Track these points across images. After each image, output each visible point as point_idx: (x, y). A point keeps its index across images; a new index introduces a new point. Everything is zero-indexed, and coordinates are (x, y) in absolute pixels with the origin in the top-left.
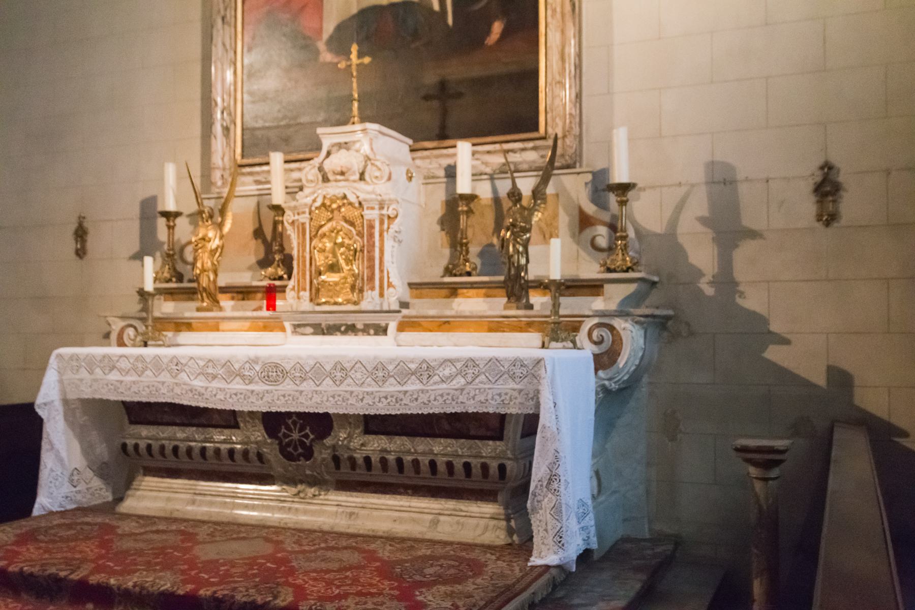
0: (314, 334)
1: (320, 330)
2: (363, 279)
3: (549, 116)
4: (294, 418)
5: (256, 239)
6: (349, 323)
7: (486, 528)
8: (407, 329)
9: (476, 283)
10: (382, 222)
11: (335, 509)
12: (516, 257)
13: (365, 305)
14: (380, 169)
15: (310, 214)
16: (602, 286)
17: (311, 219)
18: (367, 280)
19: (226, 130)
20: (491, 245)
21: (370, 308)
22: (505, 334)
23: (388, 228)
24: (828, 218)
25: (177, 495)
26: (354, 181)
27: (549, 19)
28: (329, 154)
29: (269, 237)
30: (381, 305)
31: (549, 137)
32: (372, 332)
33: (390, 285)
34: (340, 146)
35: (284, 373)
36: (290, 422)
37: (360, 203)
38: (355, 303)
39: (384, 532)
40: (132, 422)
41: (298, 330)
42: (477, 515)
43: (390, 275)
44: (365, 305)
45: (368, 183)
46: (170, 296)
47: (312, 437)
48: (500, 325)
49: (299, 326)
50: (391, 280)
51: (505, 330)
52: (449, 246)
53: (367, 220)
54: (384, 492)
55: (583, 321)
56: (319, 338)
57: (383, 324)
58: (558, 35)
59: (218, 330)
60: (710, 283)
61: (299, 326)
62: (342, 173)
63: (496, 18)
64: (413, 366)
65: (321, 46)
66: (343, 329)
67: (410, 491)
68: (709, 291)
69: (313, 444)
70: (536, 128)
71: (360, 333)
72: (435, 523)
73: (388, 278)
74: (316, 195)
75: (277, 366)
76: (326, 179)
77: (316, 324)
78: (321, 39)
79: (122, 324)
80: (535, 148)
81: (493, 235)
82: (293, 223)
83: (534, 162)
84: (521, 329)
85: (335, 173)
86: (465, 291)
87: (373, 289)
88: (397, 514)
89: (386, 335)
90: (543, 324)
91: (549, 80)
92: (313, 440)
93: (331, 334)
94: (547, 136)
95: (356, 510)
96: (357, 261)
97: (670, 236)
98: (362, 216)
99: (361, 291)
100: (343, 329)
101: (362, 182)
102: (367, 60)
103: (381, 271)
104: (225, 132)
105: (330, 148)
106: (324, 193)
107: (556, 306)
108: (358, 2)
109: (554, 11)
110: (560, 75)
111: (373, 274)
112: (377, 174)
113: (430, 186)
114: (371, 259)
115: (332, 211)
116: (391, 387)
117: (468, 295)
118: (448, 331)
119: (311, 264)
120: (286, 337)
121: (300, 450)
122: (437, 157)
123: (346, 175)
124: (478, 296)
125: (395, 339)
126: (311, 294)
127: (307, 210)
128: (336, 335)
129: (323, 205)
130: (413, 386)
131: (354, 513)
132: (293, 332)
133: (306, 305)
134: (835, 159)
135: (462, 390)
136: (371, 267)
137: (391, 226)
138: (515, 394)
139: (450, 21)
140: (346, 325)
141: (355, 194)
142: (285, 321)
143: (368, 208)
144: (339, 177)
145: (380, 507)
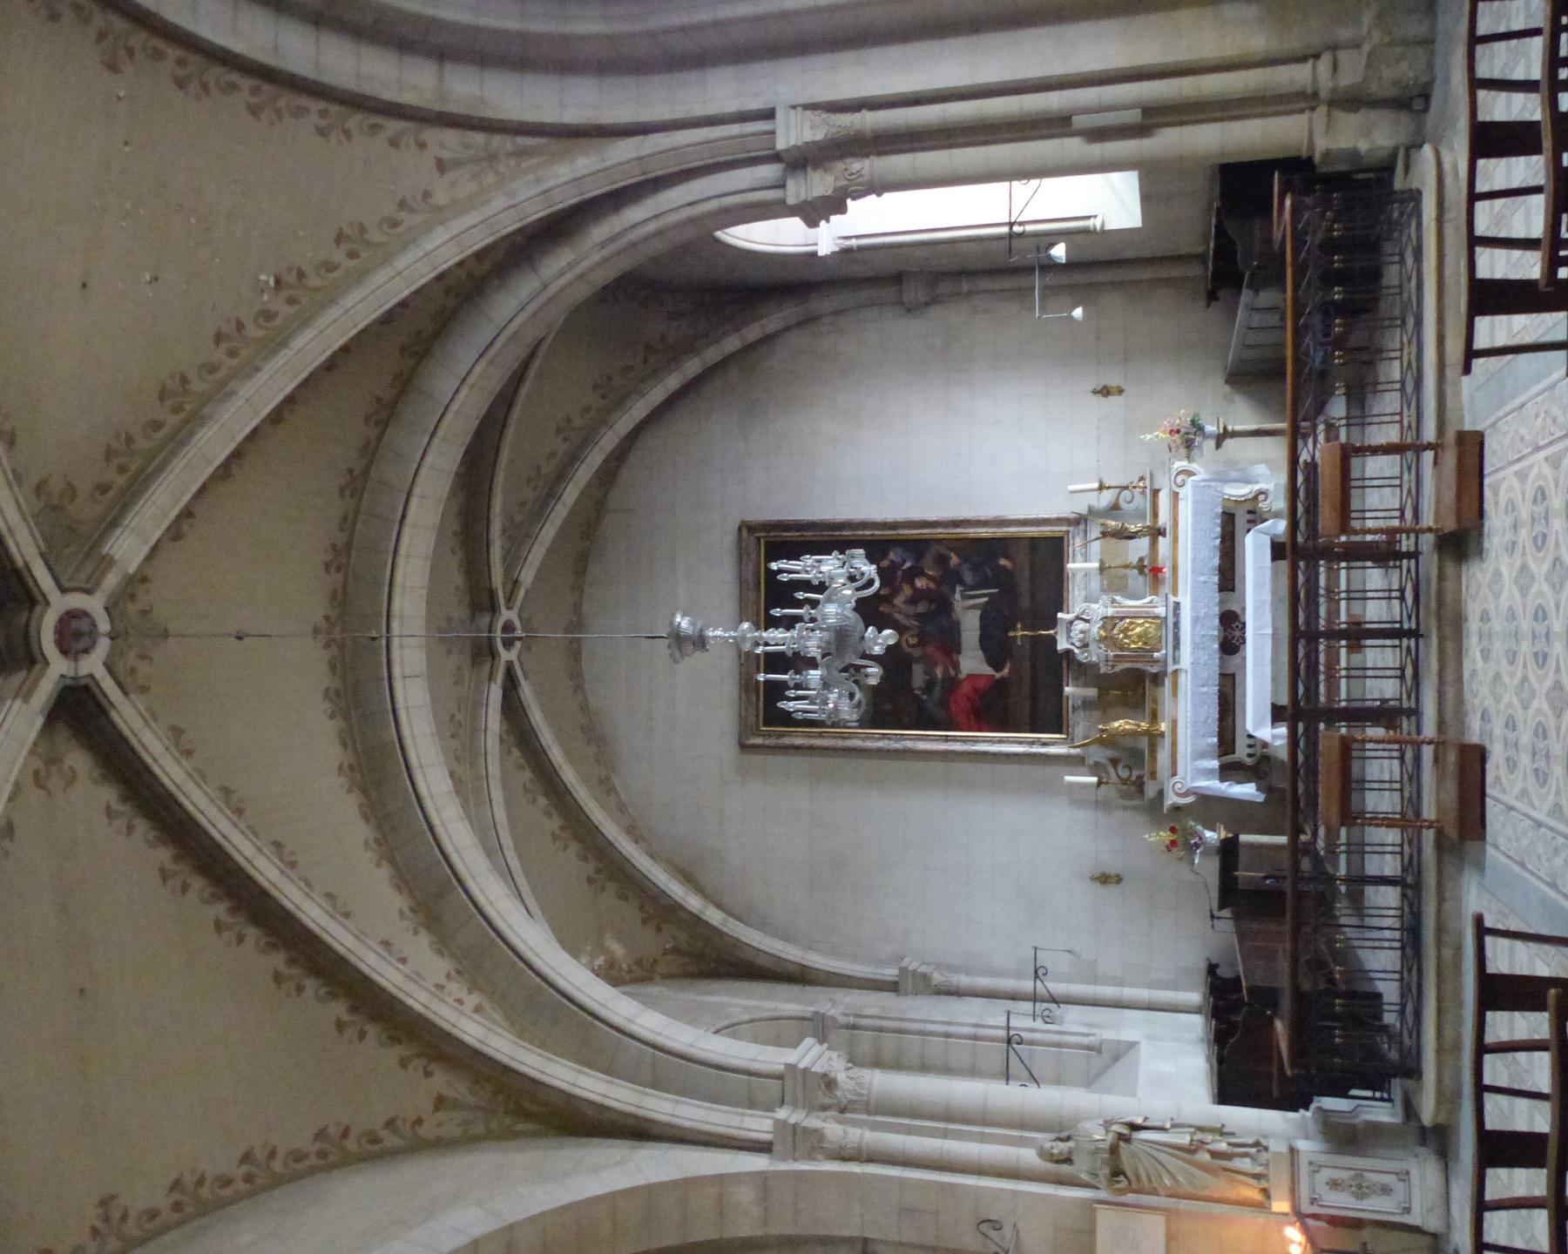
10: (1115, 607)
24: (1120, 391)
33: (1151, 602)
40: (1234, 753)
56: (1182, 647)
61: (1174, 659)
65: (998, 675)
80: (1073, 539)
82: (1113, 666)
102: (1019, 626)
103: (1143, 607)
134: (1092, 389)
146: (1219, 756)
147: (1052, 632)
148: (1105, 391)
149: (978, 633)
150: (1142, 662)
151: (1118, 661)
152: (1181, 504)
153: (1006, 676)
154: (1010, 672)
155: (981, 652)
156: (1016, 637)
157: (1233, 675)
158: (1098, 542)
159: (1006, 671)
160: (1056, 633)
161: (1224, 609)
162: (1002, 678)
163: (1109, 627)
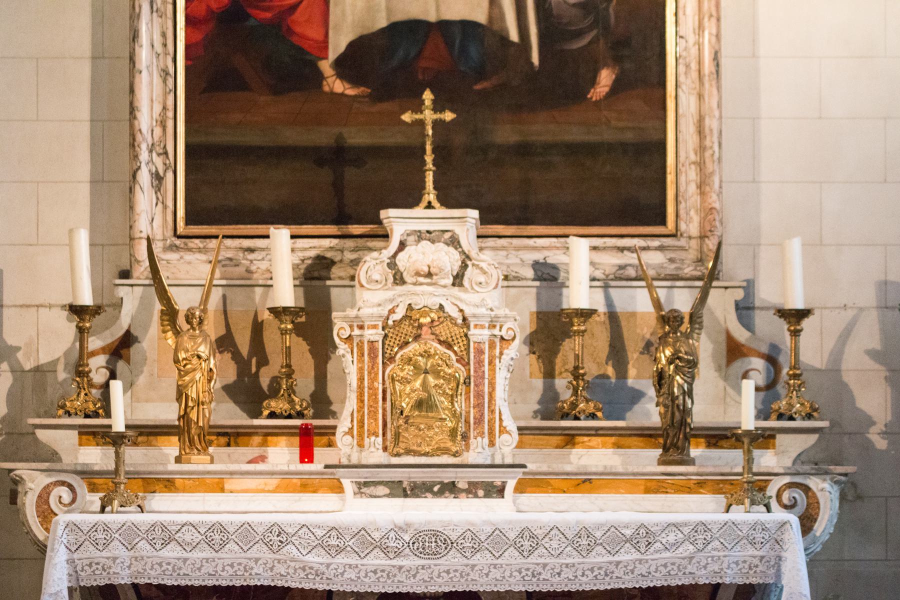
0: (391, 495)
1: (399, 490)
2: (467, 422)
3: (682, 206)
5: (220, 352)
6: (446, 481)
8: (529, 489)
9: (602, 428)
10: (492, 346)
12: (681, 397)
14: (485, 273)
15: (383, 329)
16: (773, 437)
17: (386, 336)
18: (475, 423)
19: (158, 178)
20: (605, 376)
21: (480, 461)
22: (668, 495)
23: (501, 354)
26: (445, 287)
27: (682, 79)
28: (402, 246)
29: (244, 349)
30: (493, 456)
31: (681, 235)
32: (481, 493)
33: (503, 430)
34: (420, 236)
35: (448, 544)
37: (464, 319)
41: (364, 490)
43: (503, 418)
44: (471, 457)
45: (466, 291)
46: (91, 438)
48: (659, 484)
49: (366, 484)
50: (504, 424)
51: (668, 490)
52: (542, 375)
53: (475, 342)
55: (771, 480)
56: (399, 502)
58: (693, 100)
59: (222, 490)
60: (884, 434)
61: (366, 484)
62: (429, 275)
63: (606, 65)
64: (628, 532)
65: (326, 67)
66: (436, 489)
68: (881, 444)
70: (663, 222)
71: (464, 494)
73: (501, 420)
74: (395, 304)
75: (436, 534)
76: (399, 279)
77: (393, 482)
78: (326, 58)
79: (44, 480)
80: (661, 248)
81: (607, 363)
82: (349, 338)
83: (661, 266)
84: (689, 490)
85: (418, 274)
86: (586, 439)
87: (482, 434)
89: (503, 497)
90: (718, 484)
91: (682, 158)
93: (418, 496)
94: (679, 233)
96: (459, 397)
97: (834, 371)
98: (466, 335)
99: (465, 437)
100: (436, 489)
101: (456, 288)
102: (449, 116)
103: (492, 412)
104: (155, 183)
105: (405, 237)
107: (749, 461)
108: (389, 10)
109: (688, 66)
110: (696, 154)
111: (482, 415)
112: (482, 279)
113: (512, 290)
114: (479, 395)
115: (420, 326)
116: (600, 557)
117: (590, 444)
119: (384, 399)
120: (343, 500)
122: (518, 249)
123: (434, 277)
124: (604, 446)
125: (514, 502)
126: (384, 440)
127: (380, 324)
128: (426, 497)
129: (406, 317)
130: (627, 555)
132: (355, 494)
133: (377, 455)
135: (691, 558)
136: (479, 406)
137: (505, 351)
138: (756, 561)
139: (535, 58)
140: (441, 483)
141: (458, 307)
142: (344, 478)
143: (476, 326)
144: (421, 279)
146: (135, 586)
147: (431, 195)
149: (432, 18)
150: (360, 408)
153: (326, 89)
154: (333, 94)
155: (382, 23)
156: (418, 108)
158: (651, 309)
159: (339, 86)
160: (429, 206)
162: (319, 77)
163: (444, 331)
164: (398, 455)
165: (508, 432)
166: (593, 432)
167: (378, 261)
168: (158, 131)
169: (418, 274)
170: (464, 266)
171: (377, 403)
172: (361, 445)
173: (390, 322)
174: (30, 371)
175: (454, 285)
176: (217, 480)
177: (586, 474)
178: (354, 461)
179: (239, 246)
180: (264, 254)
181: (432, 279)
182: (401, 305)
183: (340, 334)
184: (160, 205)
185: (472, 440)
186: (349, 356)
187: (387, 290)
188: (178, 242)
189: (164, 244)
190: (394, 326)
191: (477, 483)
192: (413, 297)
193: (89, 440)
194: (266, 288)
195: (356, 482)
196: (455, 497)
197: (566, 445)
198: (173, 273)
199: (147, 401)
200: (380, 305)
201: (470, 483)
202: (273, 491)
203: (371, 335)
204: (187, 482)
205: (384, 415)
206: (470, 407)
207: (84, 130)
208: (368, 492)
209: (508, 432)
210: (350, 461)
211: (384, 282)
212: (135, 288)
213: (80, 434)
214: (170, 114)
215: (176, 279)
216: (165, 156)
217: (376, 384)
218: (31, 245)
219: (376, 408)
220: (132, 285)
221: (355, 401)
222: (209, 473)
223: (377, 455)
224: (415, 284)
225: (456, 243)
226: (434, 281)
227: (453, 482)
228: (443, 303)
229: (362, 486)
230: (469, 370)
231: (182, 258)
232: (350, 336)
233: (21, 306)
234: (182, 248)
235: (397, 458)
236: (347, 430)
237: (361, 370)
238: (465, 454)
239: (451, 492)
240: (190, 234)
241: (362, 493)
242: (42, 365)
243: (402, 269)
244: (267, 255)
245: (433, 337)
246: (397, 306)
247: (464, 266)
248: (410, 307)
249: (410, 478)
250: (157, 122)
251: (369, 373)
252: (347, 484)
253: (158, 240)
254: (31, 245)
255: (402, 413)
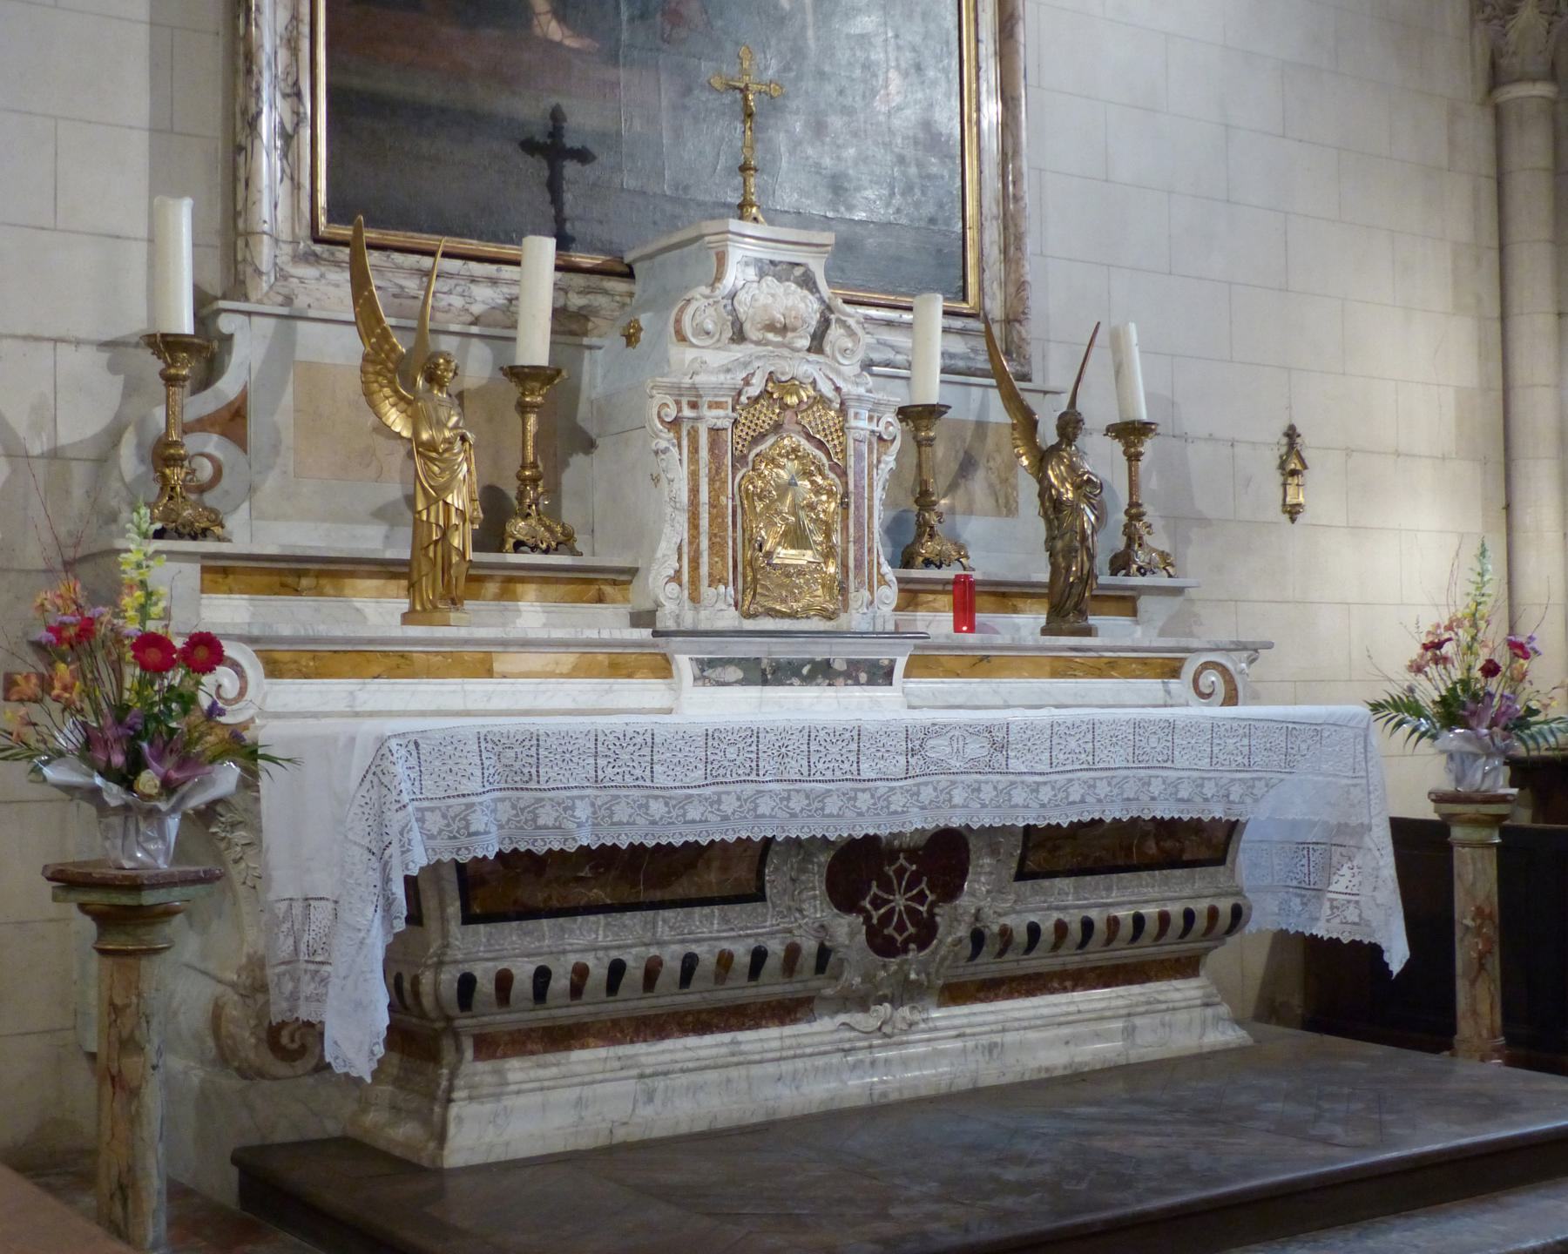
0: (745, 682)
4: (902, 861)
6: (819, 658)
7: (1204, 1022)
11: (959, 1044)
13: (856, 619)
15: (734, 410)
17: (736, 422)
19: (288, 138)
23: (879, 462)
25: (599, 1088)
32: (863, 677)
33: (883, 581)
36: (890, 870)
37: (842, 404)
38: (830, 616)
39: (1065, 1068)
40: (468, 919)
42: (1183, 1004)
46: (219, 578)
47: (931, 897)
53: (855, 440)
54: (1030, 993)
56: (754, 692)
57: (884, 659)
59: (490, 674)
61: (713, 663)
66: (805, 671)
67: (1068, 984)
69: (937, 910)
72: (1130, 1032)
82: (675, 424)
85: (771, 327)
86: (931, 597)
88: (1065, 1031)
89: (891, 684)
92: (933, 905)
93: (780, 683)
95: (997, 1038)
98: (842, 429)
99: (844, 590)
100: (805, 671)
101: (813, 357)
106: (772, 369)
117: (936, 605)
118: (988, 674)
121: (911, 930)
123: (790, 335)
127: (730, 400)
128: (791, 684)
129: (766, 394)
131: (995, 1045)
132: (695, 679)
133: (729, 619)
140: (812, 661)
141: (834, 383)
144: (770, 336)
145: (1033, 1023)
148: (1293, 465)
151: (694, 450)
152: (1152, 687)
153: (538, 31)
157: (759, 896)
161: (973, 843)
164: (754, 616)
165: (887, 583)
166: (940, 588)
167: (711, 301)
168: (283, 55)
169: (771, 327)
170: (825, 323)
171: (726, 530)
172: (695, 598)
173: (743, 399)
174: (42, 456)
175: (809, 350)
176: (481, 655)
177: (983, 648)
178: (688, 624)
179: (416, 266)
180: (452, 282)
181: (784, 337)
182: (759, 375)
183: (662, 414)
184: (287, 182)
185: (852, 595)
186: (675, 450)
187: (719, 348)
188: (318, 248)
189: (295, 251)
190: (745, 407)
191: (858, 661)
192: (777, 361)
193: (216, 582)
194: (465, 339)
195: (697, 659)
196: (829, 685)
197: (908, 605)
198: (318, 300)
199: (276, 519)
200: (728, 371)
201: (850, 663)
202: (569, 676)
203: (718, 418)
204: (434, 659)
205: (734, 551)
206: (848, 542)
207: (140, 37)
208: (713, 676)
209: (887, 583)
210: (678, 625)
211: (717, 336)
212: (255, 319)
213: (204, 570)
214: (306, 29)
215: (323, 309)
216: (295, 99)
217: (723, 499)
218: (43, 229)
219: (724, 539)
220: (249, 314)
221: (686, 525)
222: (466, 642)
223: (729, 619)
224: (758, 343)
225: (811, 285)
226: (787, 340)
227: (828, 661)
228: (816, 375)
229: (707, 670)
230: (847, 483)
231: (322, 276)
232: (676, 419)
233: (26, 338)
234: (325, 260)
235: (751, 621)
236: (672, 572)
237: (694, 476)
238: (843, 616)
239: (826, 676)
240: (339, 238)
241: (705, 678)
242: (63, 447)
243: (742, 317)
244: (456, 285)
245: (799, 428)
246: (753, 374)
247: (825, 323)
248: (771, 377)
249: (770, 653)
250: (281, 39)
251: (712, 481)
252: (684, 664)
253: (284, 242)
254: (43, 229)
255: (761, 547)
